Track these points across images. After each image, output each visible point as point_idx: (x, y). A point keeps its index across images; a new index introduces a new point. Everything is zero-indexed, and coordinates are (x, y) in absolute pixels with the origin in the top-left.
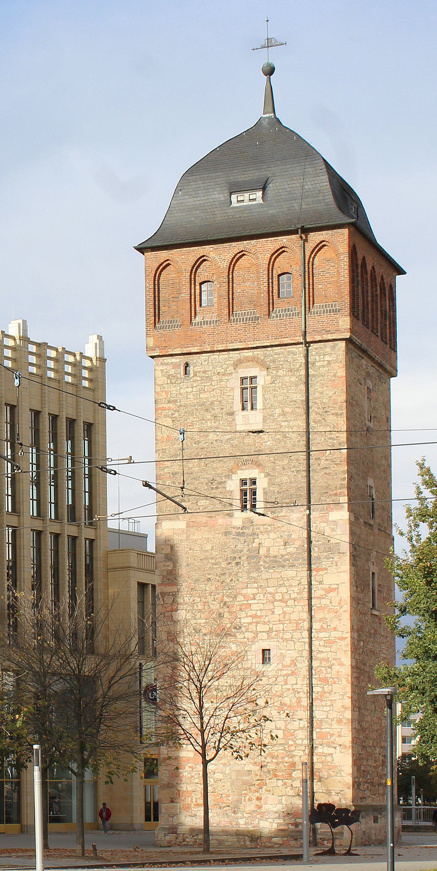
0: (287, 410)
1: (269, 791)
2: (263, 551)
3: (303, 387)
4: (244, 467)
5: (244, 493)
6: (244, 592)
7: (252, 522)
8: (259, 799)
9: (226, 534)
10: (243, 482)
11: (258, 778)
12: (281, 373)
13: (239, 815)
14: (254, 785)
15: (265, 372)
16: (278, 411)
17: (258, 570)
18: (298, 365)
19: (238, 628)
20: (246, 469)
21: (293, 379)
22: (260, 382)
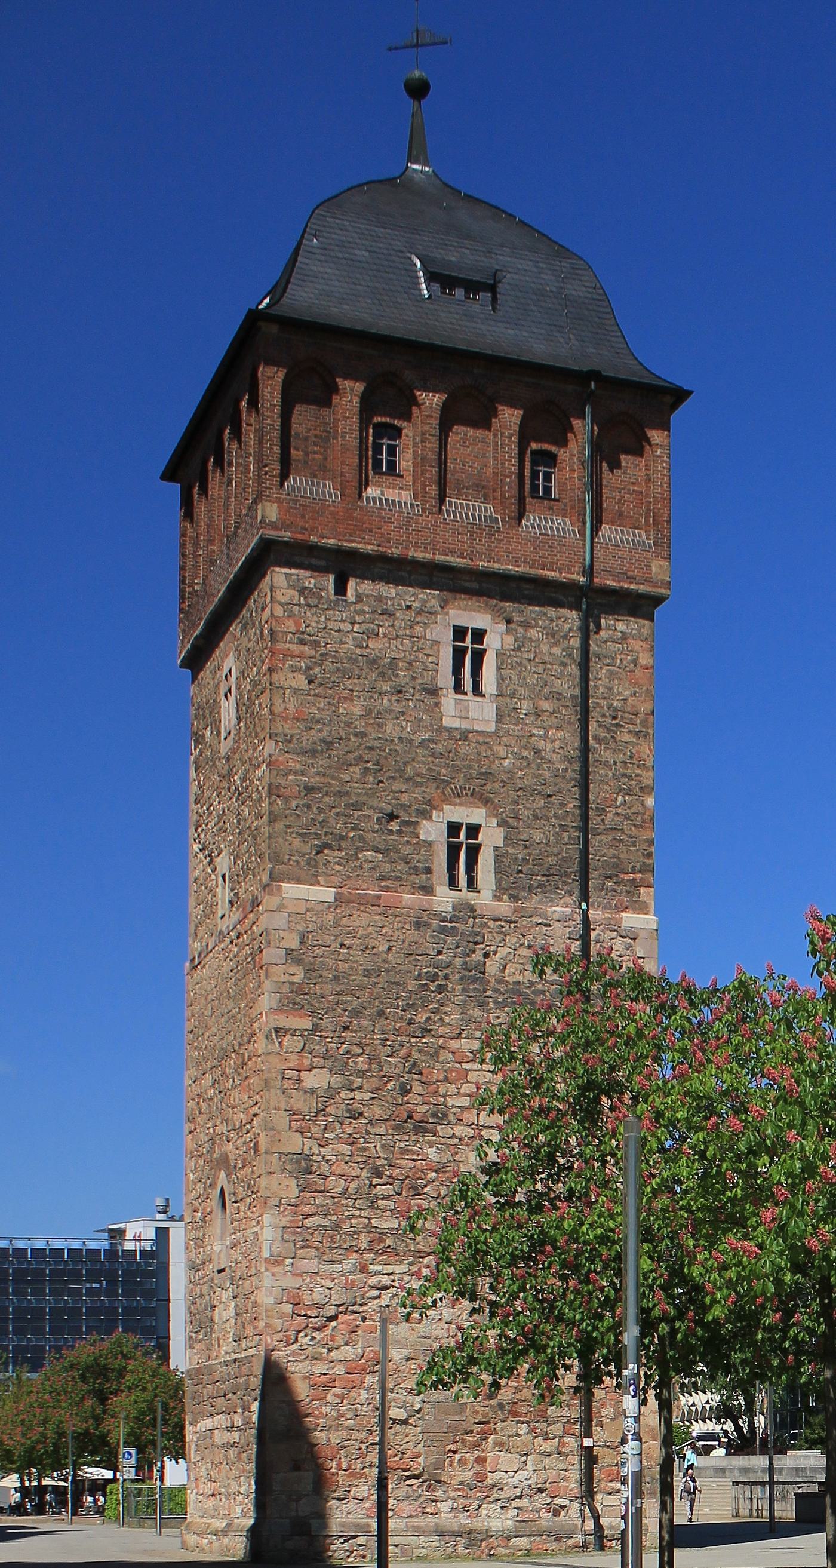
0: (546, 705)
1: (502, 1444)
2: (492, 967)
3: (574, 669)
4: (457, 800)
5: (453, 851)
6: (454, 1044)
7: (473, 910)
8: (481, 1461)
9: (418, 925)
10: (453, 829)
11: (479, 1418)
12: (533, 633)
13: (440, 1493)
14: (471, 1432)
15: (503, 627)
16: (525, 706)
17: (483, 1005)
18: (567, 627)
19: (441, 1116)
20: (461, 805)
21: (556, 651)
22: (493, 642)
